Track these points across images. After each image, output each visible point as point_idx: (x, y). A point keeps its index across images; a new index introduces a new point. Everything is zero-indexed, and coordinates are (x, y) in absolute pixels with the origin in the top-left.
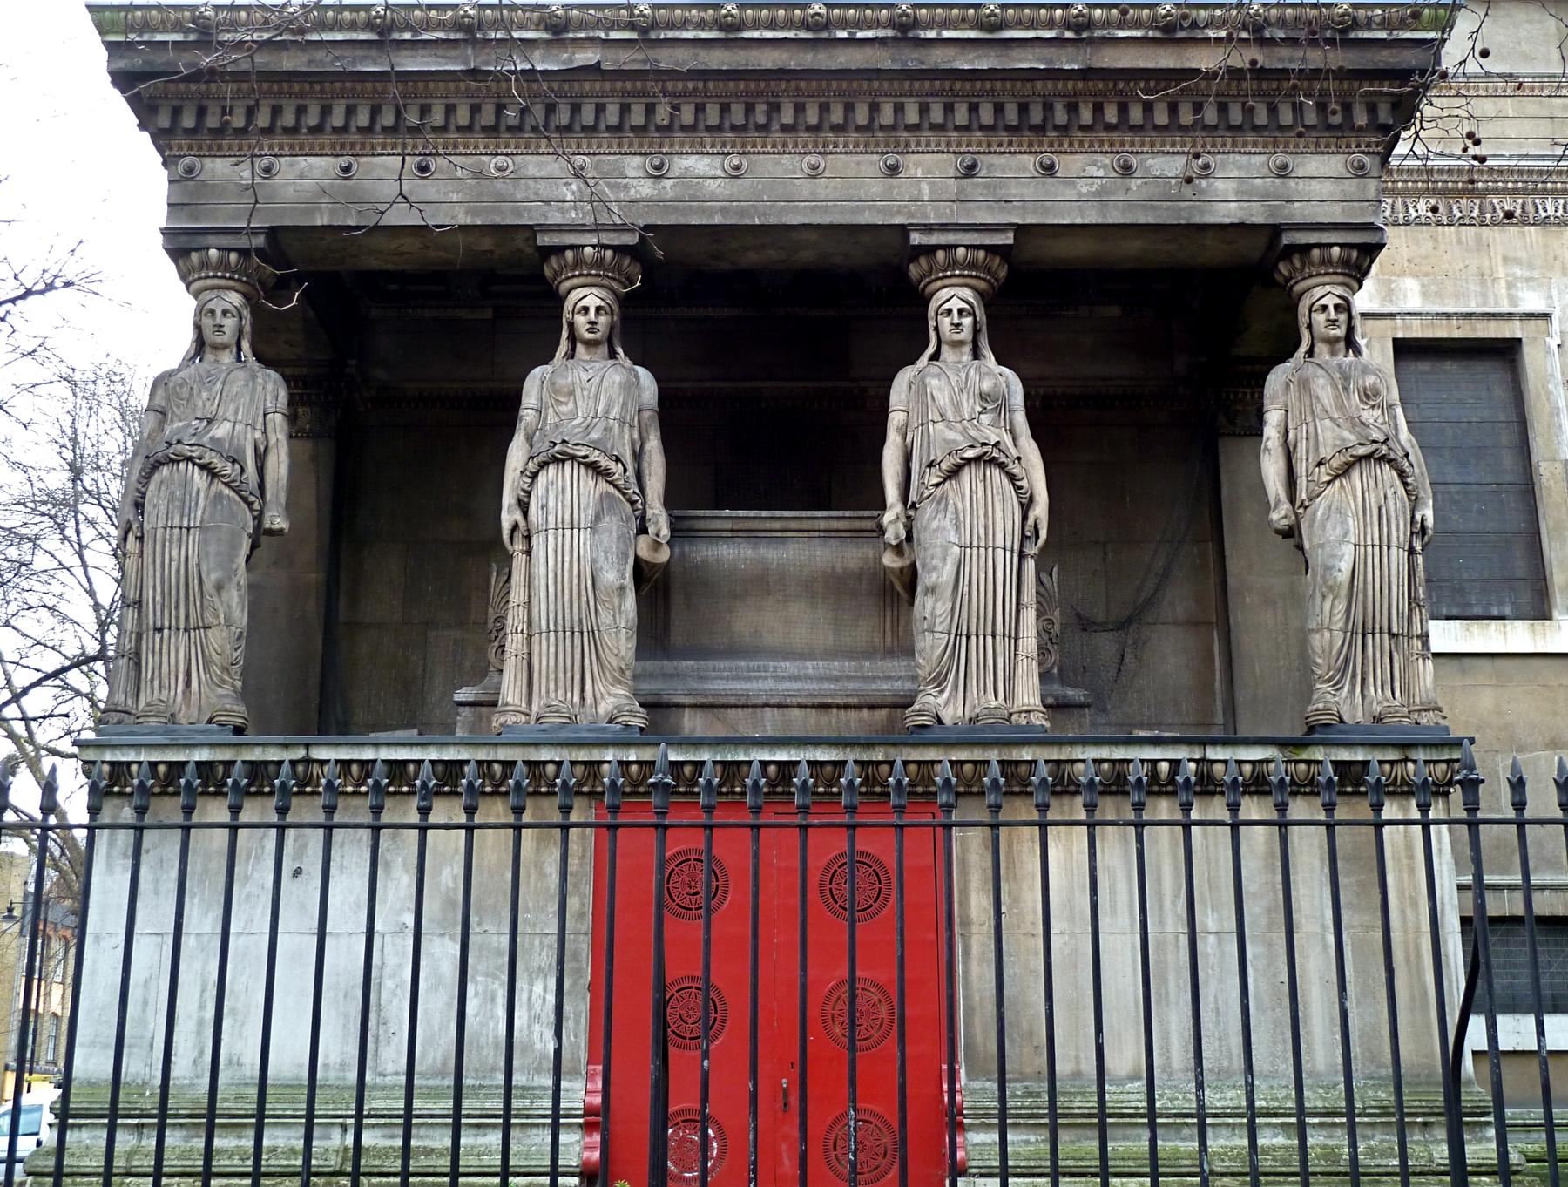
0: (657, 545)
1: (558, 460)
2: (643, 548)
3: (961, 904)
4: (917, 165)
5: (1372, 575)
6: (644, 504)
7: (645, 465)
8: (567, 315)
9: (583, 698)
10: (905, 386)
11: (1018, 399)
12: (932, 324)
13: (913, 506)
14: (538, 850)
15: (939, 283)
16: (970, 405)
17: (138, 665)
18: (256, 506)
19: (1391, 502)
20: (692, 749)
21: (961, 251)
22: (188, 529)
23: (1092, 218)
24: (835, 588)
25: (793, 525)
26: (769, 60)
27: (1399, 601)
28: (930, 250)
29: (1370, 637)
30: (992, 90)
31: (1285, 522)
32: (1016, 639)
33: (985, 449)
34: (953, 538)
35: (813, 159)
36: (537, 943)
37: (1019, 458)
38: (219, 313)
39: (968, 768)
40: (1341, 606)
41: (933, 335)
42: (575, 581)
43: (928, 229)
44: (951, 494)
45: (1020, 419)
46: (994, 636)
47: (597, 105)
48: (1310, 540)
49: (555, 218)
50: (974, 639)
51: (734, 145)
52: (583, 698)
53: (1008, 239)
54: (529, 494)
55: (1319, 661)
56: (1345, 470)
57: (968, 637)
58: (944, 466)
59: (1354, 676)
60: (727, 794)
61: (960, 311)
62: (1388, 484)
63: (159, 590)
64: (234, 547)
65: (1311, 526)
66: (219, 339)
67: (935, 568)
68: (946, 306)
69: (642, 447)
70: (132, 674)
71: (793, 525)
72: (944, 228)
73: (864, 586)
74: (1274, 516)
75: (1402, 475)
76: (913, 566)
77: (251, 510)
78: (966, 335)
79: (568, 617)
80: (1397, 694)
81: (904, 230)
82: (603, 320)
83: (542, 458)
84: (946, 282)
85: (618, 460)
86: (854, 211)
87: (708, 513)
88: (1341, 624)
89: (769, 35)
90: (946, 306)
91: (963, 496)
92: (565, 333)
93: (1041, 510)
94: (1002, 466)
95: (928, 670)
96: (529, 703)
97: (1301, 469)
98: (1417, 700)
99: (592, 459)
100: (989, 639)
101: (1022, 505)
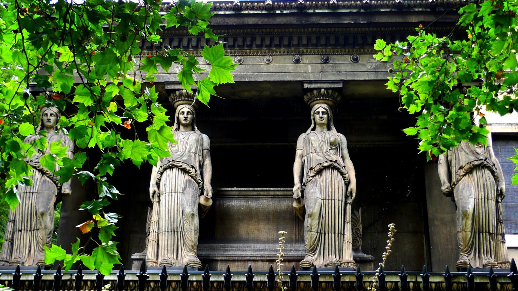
0: (207, 199)
1: (171, 167)
2: (202, 200)
4: (306, 59)
5: (482, 211)
6: (203, 184)
7: (204, 169)
8: (177, 115)
9: (177, 257)
10: (302, 140)
11: (345, 145)
12: (312, 117)
13: (304, 185)
15: (315, 102)
16: (326, 147)
17: (12, 244)
18: (59, 185)
19: (488, 183)
20: (217, 276)
21: (323, 90)
22: (33, 193)
23: (372, 77)
24: (277, 218)
25: (261, 193)
26: (251, 21)
27: (493, 221)
28: (311, 90)
29: (481, 234)
30: (334, 31)
31: (447, 190)
32: (344, 235)
33: (331, 163)
34: (319, 196)
35: (268, 57)
37: (344, 166)
38: (49, 115)
40: (470, 222)
41: (313, 122)
42: (176, 212)
43: (310, 82)
44: (318, 180)
45: (346, 152)
46: (335, 233)
47: (188, 38)
48: (457, 197)
49: (172, 79)
50: (327, 234)
51: (239, 53)
52: (177, 257)
53: (340, 85)
54: (160, 180)
55: (462, 243)
56: (469, 172)
57: (325, 234)
58: (316, 169)
59: (475, 250)
61: (323, 113)
62: (487, 176)
63: (21, 216)
64: (49, 200)
65: (457, 192)
66: (49, 124)
67: (312, 207)
68: (317, 110)
69: (203, 163)
70: (10, 247)
71: (261, 193)
72: (316, 82)
73: (288, 216)
74: (443, 188)
75: (493, 173)
76: (304, 206)
77: (57, 186)
78: (325, 121)
79: (172, 226)
80: (493, 256)
81: (302, 83)
82: (190, 116)
83: (165, 167)
84: (318, 102)
85: (193, 167)
86: (283, 76)
87: (230, 189)
88: (470, 229)
89: (251, 12)
90: (317, 110)
91: (323, 180)
92: (176, 122)
93: (353, 185)
94: (338, 170)
95: (309, 246)
96: (157, 259)
97: (453, 170)
98: (501, 258)
99: (183, 167)
100: (333, 234)
101: (345, 183)
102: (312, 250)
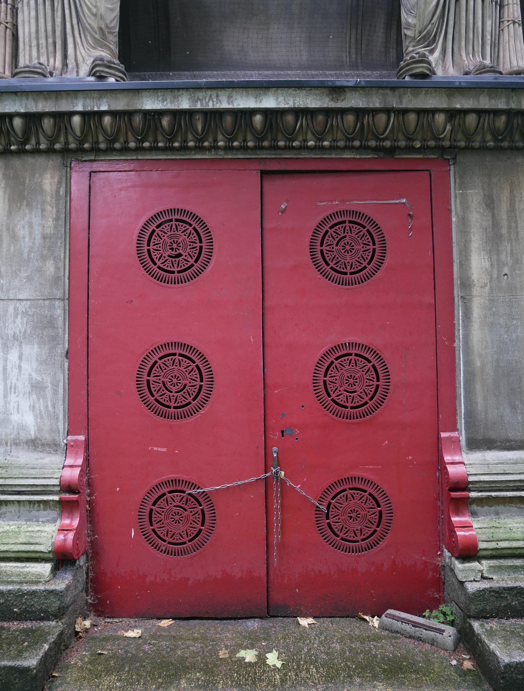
3: (461, 265)
14: (10, 212)
20: (169, 96)
36: (11, 309)
39: (471, 120)
52: (65, 65)
60: (210, 149)
95: (418, 29)
102: (424, 38)
